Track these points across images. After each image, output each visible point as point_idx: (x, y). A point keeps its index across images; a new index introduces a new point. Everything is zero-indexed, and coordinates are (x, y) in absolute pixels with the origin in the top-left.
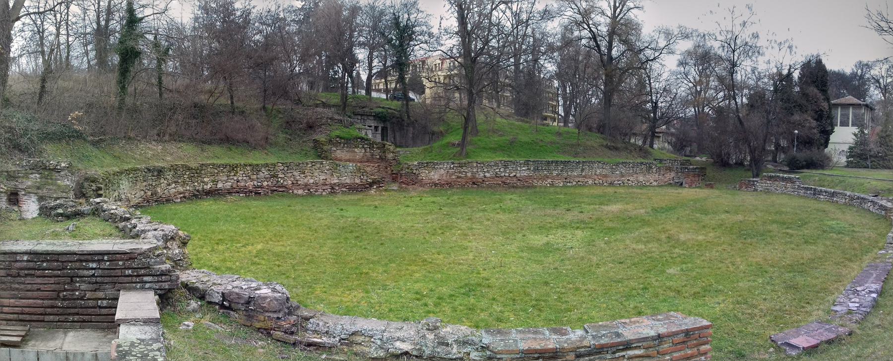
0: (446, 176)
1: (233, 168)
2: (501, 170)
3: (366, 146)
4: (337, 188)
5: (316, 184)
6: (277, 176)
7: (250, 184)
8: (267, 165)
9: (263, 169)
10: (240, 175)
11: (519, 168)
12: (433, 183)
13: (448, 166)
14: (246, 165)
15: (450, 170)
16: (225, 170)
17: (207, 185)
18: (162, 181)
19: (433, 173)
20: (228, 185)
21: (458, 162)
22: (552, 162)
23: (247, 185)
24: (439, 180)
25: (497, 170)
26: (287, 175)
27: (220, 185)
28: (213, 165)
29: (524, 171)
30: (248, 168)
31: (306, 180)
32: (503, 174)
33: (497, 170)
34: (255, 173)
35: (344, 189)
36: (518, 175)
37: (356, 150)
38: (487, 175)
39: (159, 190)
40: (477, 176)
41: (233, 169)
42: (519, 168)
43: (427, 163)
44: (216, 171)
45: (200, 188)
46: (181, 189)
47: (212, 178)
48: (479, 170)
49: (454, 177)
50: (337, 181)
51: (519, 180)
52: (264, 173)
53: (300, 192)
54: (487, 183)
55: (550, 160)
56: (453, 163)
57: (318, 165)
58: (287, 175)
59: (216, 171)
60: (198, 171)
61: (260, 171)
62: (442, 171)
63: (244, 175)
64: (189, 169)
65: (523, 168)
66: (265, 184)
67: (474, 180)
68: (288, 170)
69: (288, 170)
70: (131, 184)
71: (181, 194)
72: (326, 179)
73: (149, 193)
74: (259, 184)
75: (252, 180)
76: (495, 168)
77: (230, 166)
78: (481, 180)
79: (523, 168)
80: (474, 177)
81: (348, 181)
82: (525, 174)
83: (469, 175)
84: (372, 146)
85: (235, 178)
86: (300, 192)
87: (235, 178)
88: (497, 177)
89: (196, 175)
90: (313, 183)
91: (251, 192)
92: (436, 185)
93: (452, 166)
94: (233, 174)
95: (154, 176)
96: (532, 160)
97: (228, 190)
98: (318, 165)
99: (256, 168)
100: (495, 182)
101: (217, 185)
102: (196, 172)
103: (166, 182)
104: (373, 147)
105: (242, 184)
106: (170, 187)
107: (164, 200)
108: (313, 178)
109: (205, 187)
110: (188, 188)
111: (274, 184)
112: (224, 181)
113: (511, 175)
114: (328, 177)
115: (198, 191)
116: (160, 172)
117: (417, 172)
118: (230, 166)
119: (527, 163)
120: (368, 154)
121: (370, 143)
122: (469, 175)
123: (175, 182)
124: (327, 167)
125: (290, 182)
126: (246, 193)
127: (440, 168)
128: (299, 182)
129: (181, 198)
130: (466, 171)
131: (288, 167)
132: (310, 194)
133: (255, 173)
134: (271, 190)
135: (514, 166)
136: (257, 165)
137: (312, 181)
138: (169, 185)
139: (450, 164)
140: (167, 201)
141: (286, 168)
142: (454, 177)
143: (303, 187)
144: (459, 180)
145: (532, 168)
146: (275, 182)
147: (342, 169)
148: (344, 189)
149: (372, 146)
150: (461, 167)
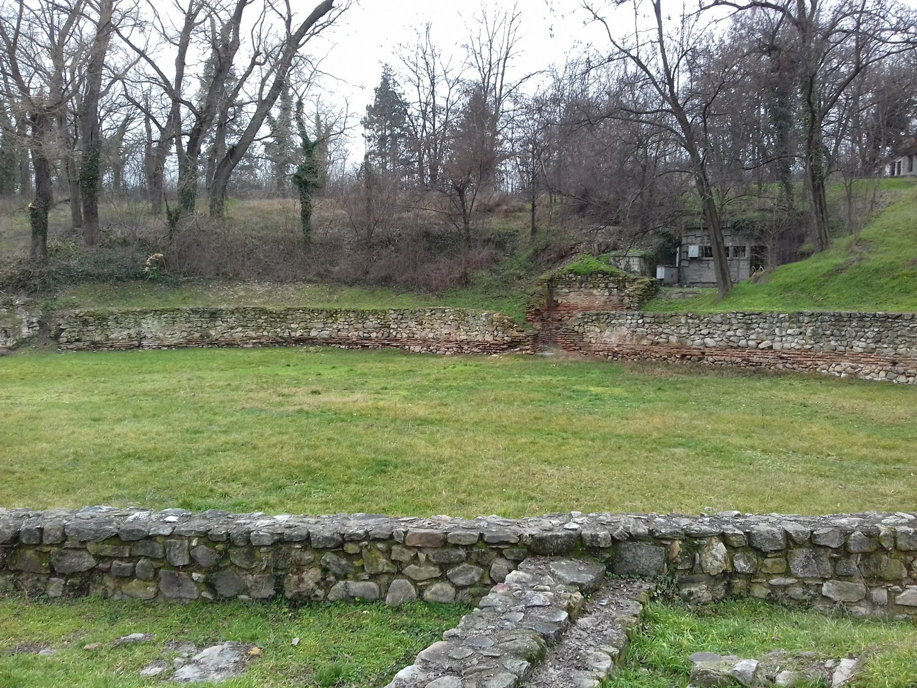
0: (631, 340)
1: (332, 314)
2: (738, 334)
3: (611, 285)
4: (466, 347)
5: (437, 340)
6: (389, 327)
7: (353, 335)
8: (375, 312)
9: (370, 317)
10: (341, 323)
11: (777, 330)
12: (609, 351)
13: (634, 321)
14: (348, 311)
15: (638, 329)
16: (320, 316)
17: (296, 332)
18: (219, 323)
19: (607, 333)
20: (325, 334)
21: (652, 314)
22: (850, 316)
23: (349, 335)
24: (618, 346)
25: (729, 333)
26: (401, 326)
27: (313, 333)
28: (304, 310)
29: (790, 338)
30: (352, 315)
31: (423, 334)
32: (743, 342)
33: (729, 333)
34: (360, 321)
35: (476, 350)
36: (777, 346)
37: (595, 291)
38: (708, 341)
39: (213, 332)
40: (689, 343)
41: (332, 316)
42: (777, 330)
43: (597, 315)
44: (308, 317)
45: (286, 335)
46: (253, 334)
47: (302, 324)
48: (692, 331)
49: (645, 342)
50: (465, 337)
51: (782, 358)
52: (372, 322)
53: (417, 349)
54: (710, 359)
55: (843, 311)
56: (642, 317)
57: (439, 314)
58: (401, 326)
59: (308, 317)
60: (282, 316)
61: (367, 319)
62: (624, 330)
63: (346, 323)
64: (264, 311)
65: (789, 331)
66: (374, 335)
67: (684, 351)
68: (401, 319)
69: (401, 319)
70: (164, 324)
71: (254, 339)
72: (450, 334)
73: (197, 335)
74: (365, 335)
75: (357, 330)
76: (725, 327)
77: (326, 311)
78: (697, 352)
79: (789, 331)
80: (681, 345)
81: (480, 338)
82: (793, 345)
83: (673, 339)
84: (621, 284)
85: (335, 326)
86: (417, 349)
87: (335, 326)
88: (731, 347)
89: (278, 320)
90: (433, 338)
91: (356, 344)
92: (615, 354)
93: (640, 321)
94: (330, 321)
95: (204, 318)
96: (807, 310)
97: (324, 339)
98: (439, 314)
99: (362, 316)
100: (728, 359)
101: (309, 332)
102: (282, 317)
103: (224, 325)
104: (624, 286)
105: (343, 334)
106: (232, 331)
107: (223, 343)
108: (433, 331)
109: (293, 334)
110: (265, 333)
111: (385, 336)
112: (319, 328)
113: (761, 346)
114: (453, 330)
115: (281, 337)
116: (214, 315)
117: (581, 330)
118: (326, 311)
119: (795, 319)
120: (615, 298)
121: (619, 281)
122: (673, 339)
123: (242, 326)
124: (452, 317)
125: (405, 335)
126: (349, 344)
127: (620, 325)
128: (416, 336)
129: (254, 343)
130: (667, 331)
131: (402, 315)
132: (432, 354)
133: (360, 321)
134: (383, 344)
135: (766, 326)
136: (363, 312)
137: (431, 335)
138: (232, 328)
139: (636, 317)
140: (227, 344)
141: (400, 317)
142: (645, 342)
143: (421, 342)
144: (656, 348)
145: (809, 331)
146: (386, 335)
147: (471, 320)
148: (476, 350)
149: (621, 284)
150: (659, 324)
